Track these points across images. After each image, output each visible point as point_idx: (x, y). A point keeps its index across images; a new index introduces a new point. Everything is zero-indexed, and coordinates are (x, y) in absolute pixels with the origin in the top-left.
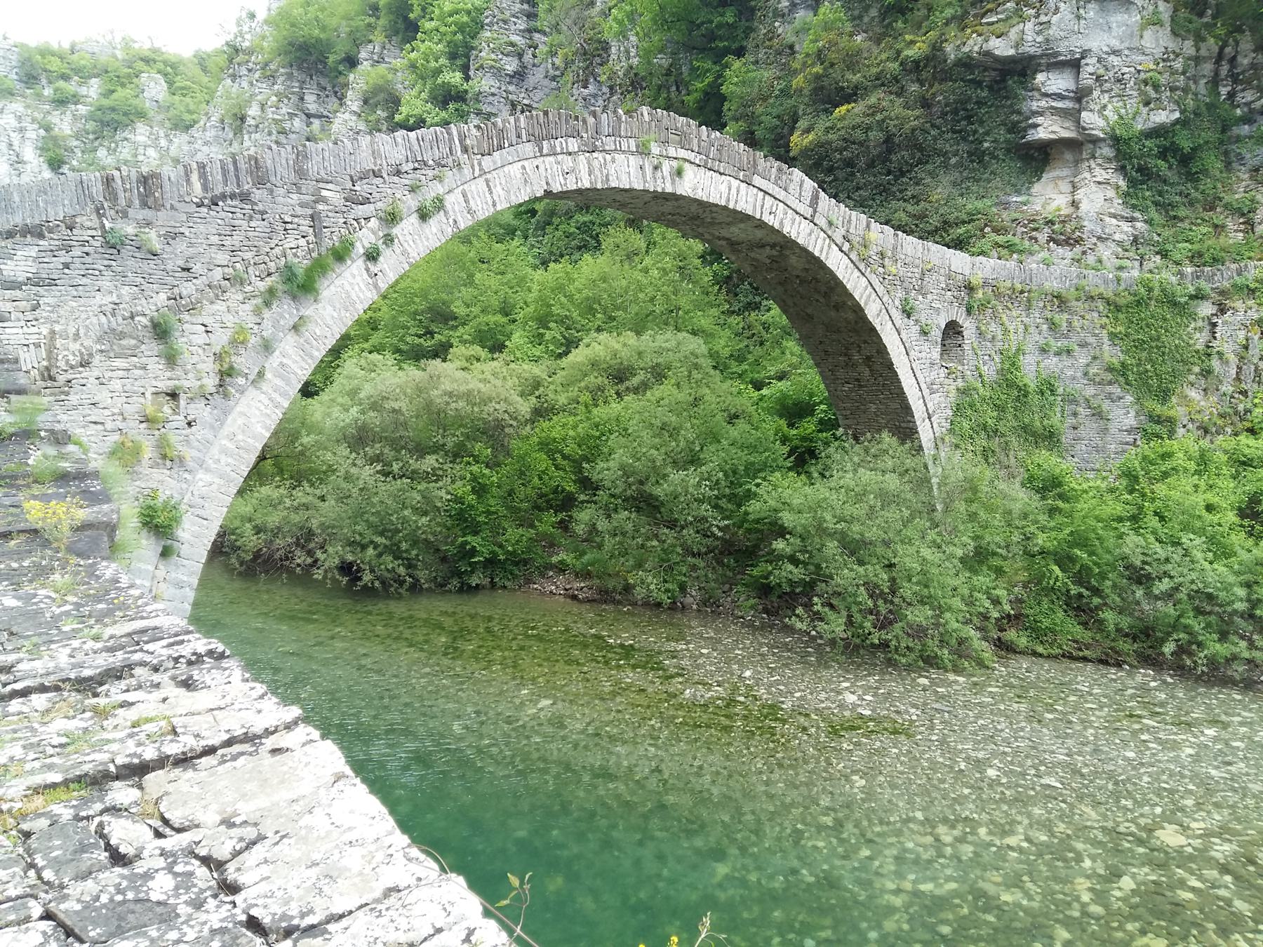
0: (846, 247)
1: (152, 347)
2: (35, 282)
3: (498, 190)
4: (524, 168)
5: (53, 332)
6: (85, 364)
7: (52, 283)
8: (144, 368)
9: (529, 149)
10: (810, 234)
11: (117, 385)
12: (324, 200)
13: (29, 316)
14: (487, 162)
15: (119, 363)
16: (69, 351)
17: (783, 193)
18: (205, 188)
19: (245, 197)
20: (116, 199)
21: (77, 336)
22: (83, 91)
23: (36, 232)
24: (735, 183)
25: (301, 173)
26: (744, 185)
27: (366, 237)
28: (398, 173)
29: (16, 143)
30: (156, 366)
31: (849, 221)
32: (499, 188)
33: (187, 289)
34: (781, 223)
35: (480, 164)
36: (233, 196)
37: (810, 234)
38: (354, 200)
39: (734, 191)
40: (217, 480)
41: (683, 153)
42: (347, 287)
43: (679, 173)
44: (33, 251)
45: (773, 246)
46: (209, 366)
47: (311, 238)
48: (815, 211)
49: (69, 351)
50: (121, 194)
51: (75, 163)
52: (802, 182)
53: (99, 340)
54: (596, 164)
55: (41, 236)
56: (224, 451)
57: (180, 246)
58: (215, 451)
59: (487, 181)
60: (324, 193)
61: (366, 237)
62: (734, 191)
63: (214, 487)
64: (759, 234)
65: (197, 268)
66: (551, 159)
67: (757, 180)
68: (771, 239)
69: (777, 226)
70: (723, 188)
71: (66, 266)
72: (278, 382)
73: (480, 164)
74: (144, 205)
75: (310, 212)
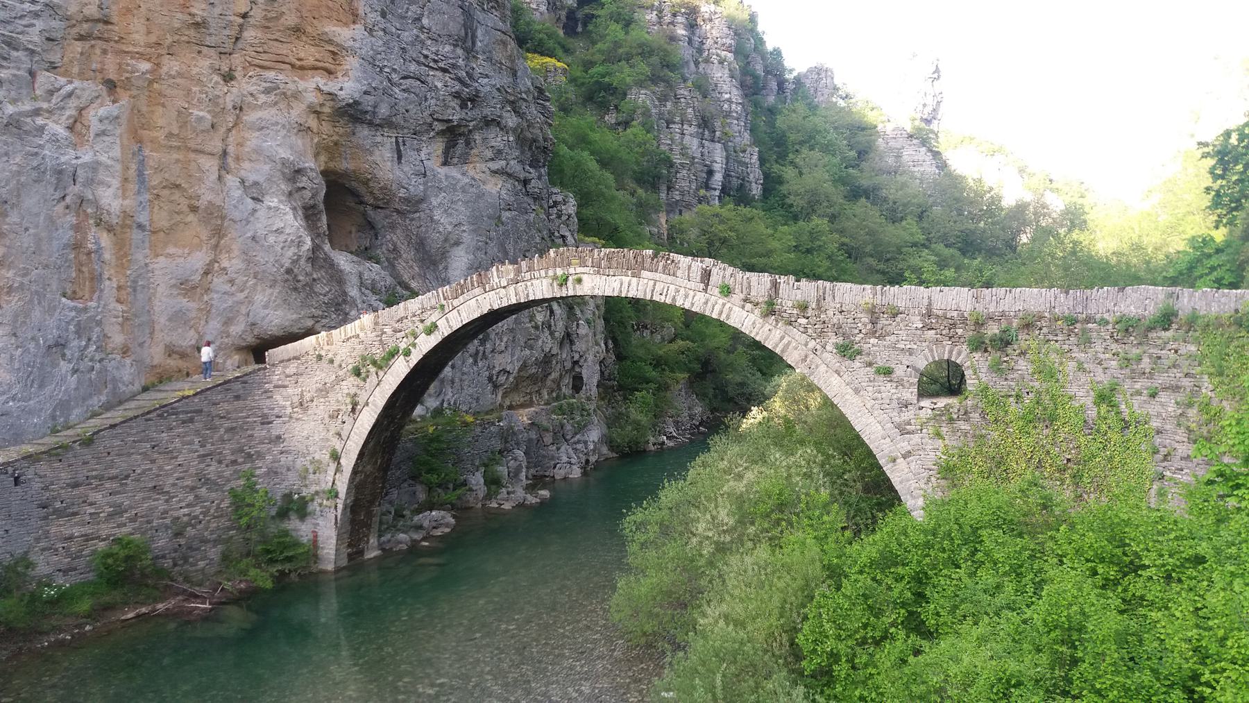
0: (749, 306)
3: (464, 314)
10: (706, 303)
14: (456, 303)
16: (307, 396)
17: (670, 278)
24: (626, 279)
26: (635, 280)
33: (341, 373)
37: (706, 303)
41: (579, 270)
43: (579, 281)
48: (707, 285)
49: (307, 396)
52: (690, 267)
61: (403, 346)
62: (625, 285)
67: (645, 274)
69: (669, 301)
70: (616, 285)
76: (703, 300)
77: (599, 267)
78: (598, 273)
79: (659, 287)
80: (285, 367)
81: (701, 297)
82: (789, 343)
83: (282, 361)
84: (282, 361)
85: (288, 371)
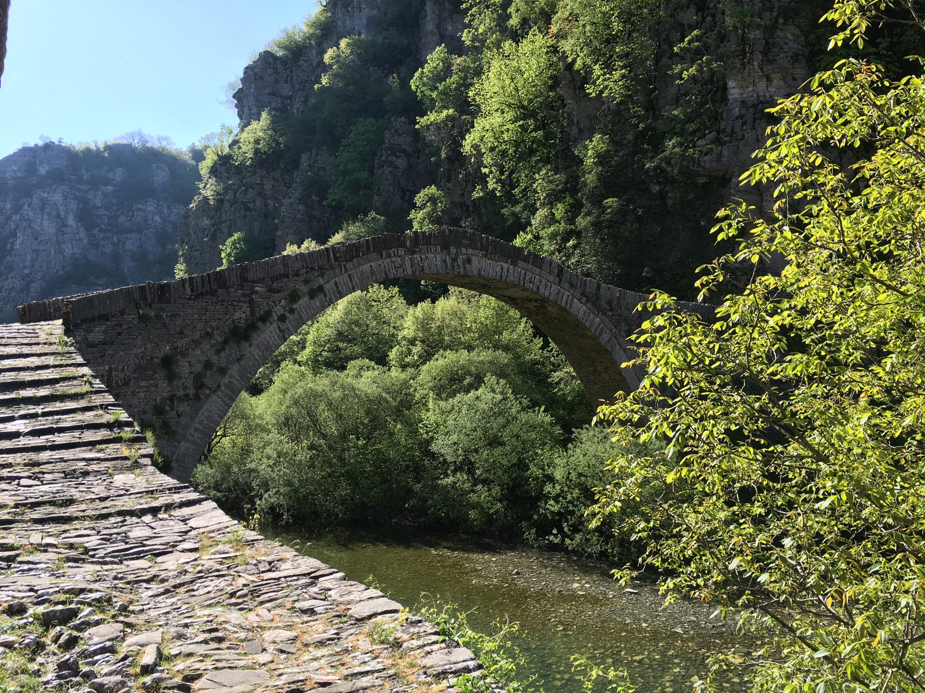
1: (161, 374)
2: (104, 343)
4: (371, 266)
5: (111, 369)
6: (126, 384)
7: (112, 343)
8: (156, 386)
9: (374, 255)
10: (558, 294)
11: (142, 395)
12: (257, 292)
13: (100, 361)
15: (143, 383)
18: (192, 290)
19: (213, 293)
20: (146, 299)
21: (123, 370)
22: (111, 175)
23: (105, 318)
24: (505, 266)
25: (244, 279)
26: (511, 267)
27: (278, 310)
28: (297, 275)
29: (63, 214)
30: (163, 384)
31: (585, 284)
32: (356, 279)
34: (538, 289)
35: (345, 266)
36: (207, 293)
37: (558, 294)
38: (271, 290)
39: (505, 271)
40: (192, 446)
41: (470, 251)
42: (268, 338)
43: (469, 261)
44: (103, 328)
45: (536, 301)
46: (189, 383)
47: (249, 313)
48: (561, 280)
50: (149, 296)
51: (103, 227)
53: (134, 372)
54: (416, 261)
55: (108, 320)
56: (197, 430)
57: (179, 321)
58: (191, 431)
59: (349, 275)
60: (257, 289)
61: (278, 310)
62: (505, 271)
63: (190, 450)
64: (526, 294)
65: (187, 332)
66: (388, 260)
67: (521, 263)
68: (534, 296)
69: (535, 289)
70: (498, 269)
71: (119, 334)
72: (228, 391)
73: (345, 266)
74: (160, 301)
75: (248, 299)
76: (556, 291)
77: (487, 252)
78: (486, 256)
79: (529, 275)
80: (89, 331)
81: (555, 288)
82: (602, 329)
83: (84, 321)
84: (84, 321)
85: (91, 337)
